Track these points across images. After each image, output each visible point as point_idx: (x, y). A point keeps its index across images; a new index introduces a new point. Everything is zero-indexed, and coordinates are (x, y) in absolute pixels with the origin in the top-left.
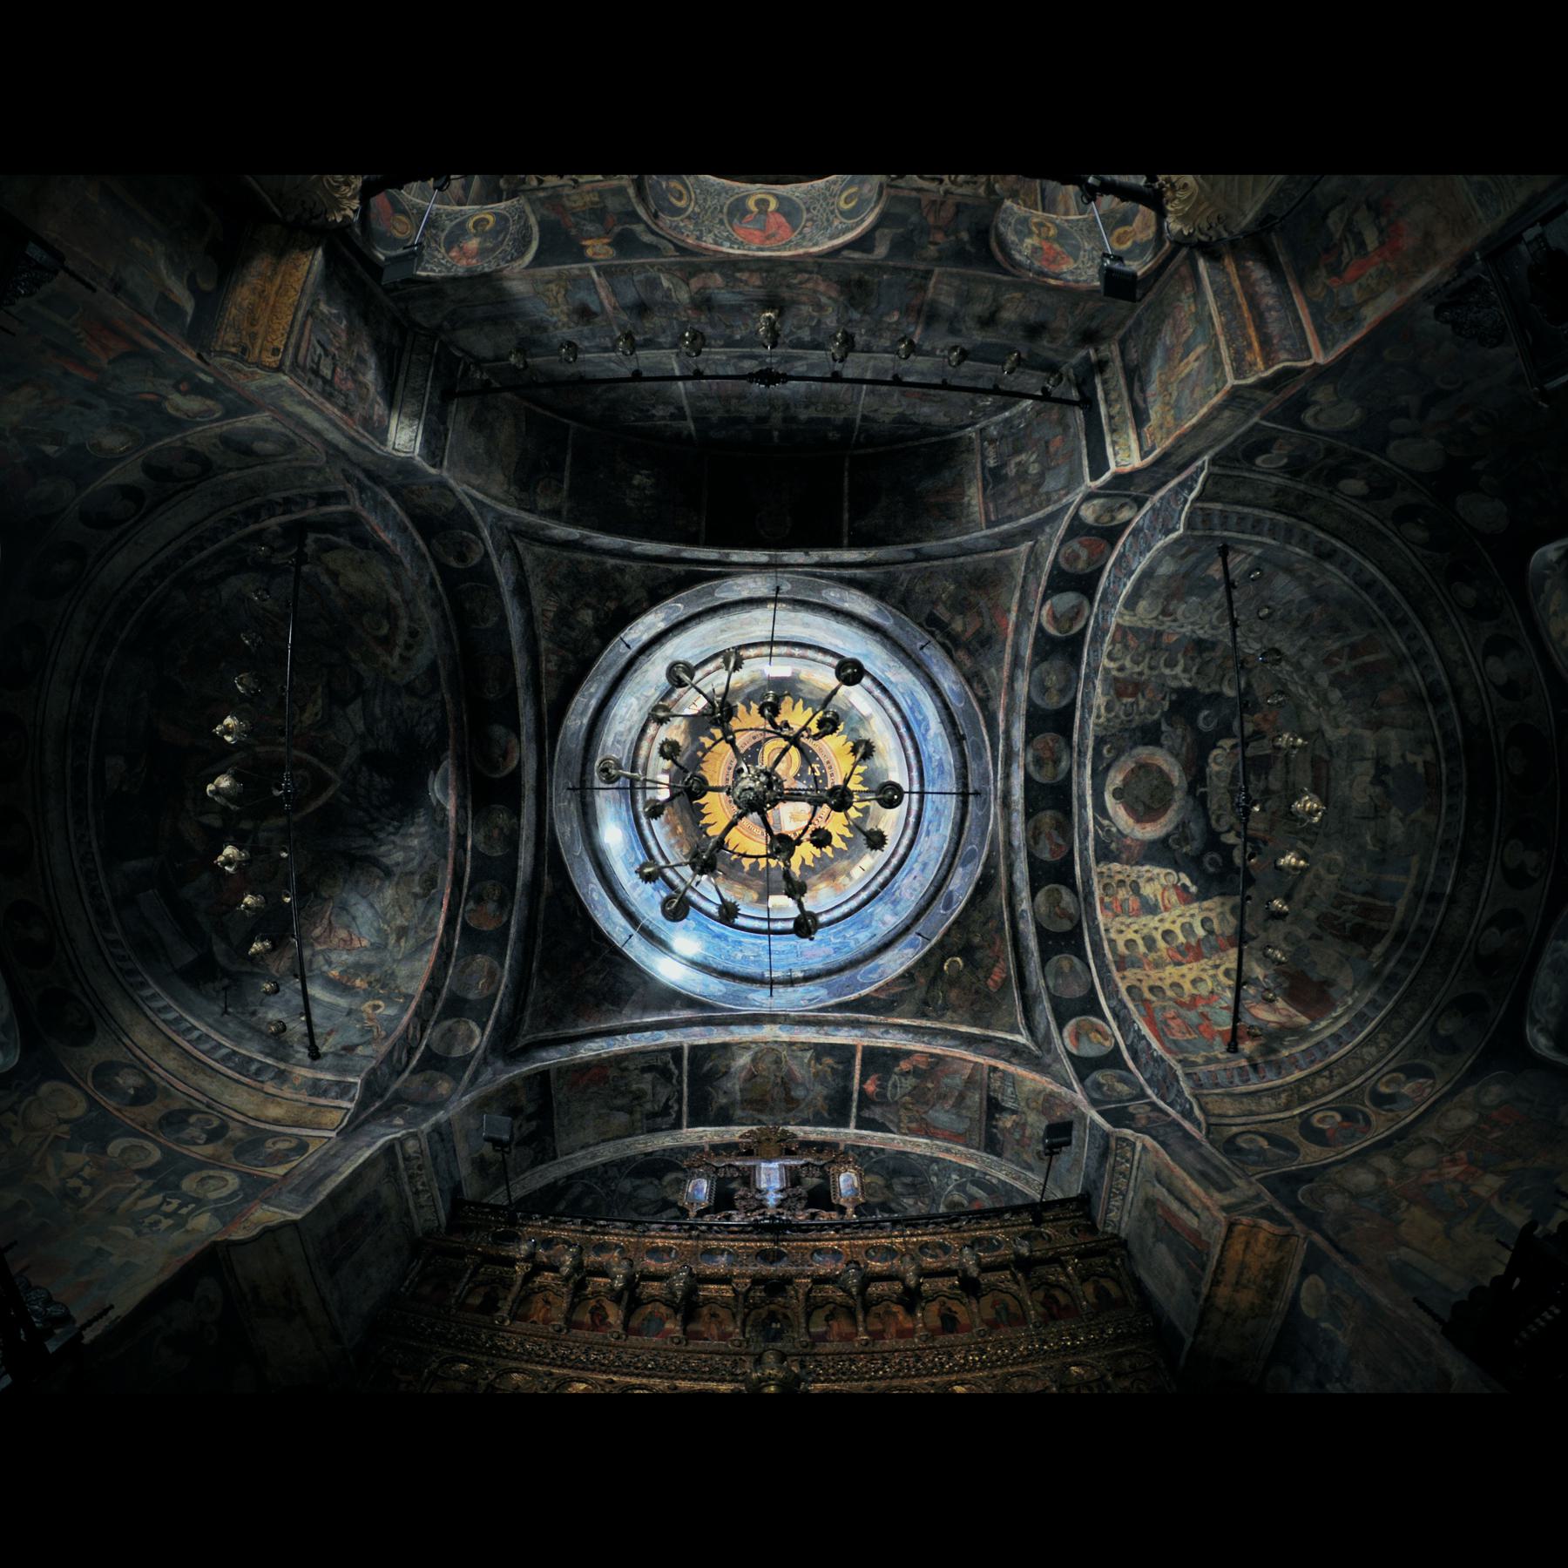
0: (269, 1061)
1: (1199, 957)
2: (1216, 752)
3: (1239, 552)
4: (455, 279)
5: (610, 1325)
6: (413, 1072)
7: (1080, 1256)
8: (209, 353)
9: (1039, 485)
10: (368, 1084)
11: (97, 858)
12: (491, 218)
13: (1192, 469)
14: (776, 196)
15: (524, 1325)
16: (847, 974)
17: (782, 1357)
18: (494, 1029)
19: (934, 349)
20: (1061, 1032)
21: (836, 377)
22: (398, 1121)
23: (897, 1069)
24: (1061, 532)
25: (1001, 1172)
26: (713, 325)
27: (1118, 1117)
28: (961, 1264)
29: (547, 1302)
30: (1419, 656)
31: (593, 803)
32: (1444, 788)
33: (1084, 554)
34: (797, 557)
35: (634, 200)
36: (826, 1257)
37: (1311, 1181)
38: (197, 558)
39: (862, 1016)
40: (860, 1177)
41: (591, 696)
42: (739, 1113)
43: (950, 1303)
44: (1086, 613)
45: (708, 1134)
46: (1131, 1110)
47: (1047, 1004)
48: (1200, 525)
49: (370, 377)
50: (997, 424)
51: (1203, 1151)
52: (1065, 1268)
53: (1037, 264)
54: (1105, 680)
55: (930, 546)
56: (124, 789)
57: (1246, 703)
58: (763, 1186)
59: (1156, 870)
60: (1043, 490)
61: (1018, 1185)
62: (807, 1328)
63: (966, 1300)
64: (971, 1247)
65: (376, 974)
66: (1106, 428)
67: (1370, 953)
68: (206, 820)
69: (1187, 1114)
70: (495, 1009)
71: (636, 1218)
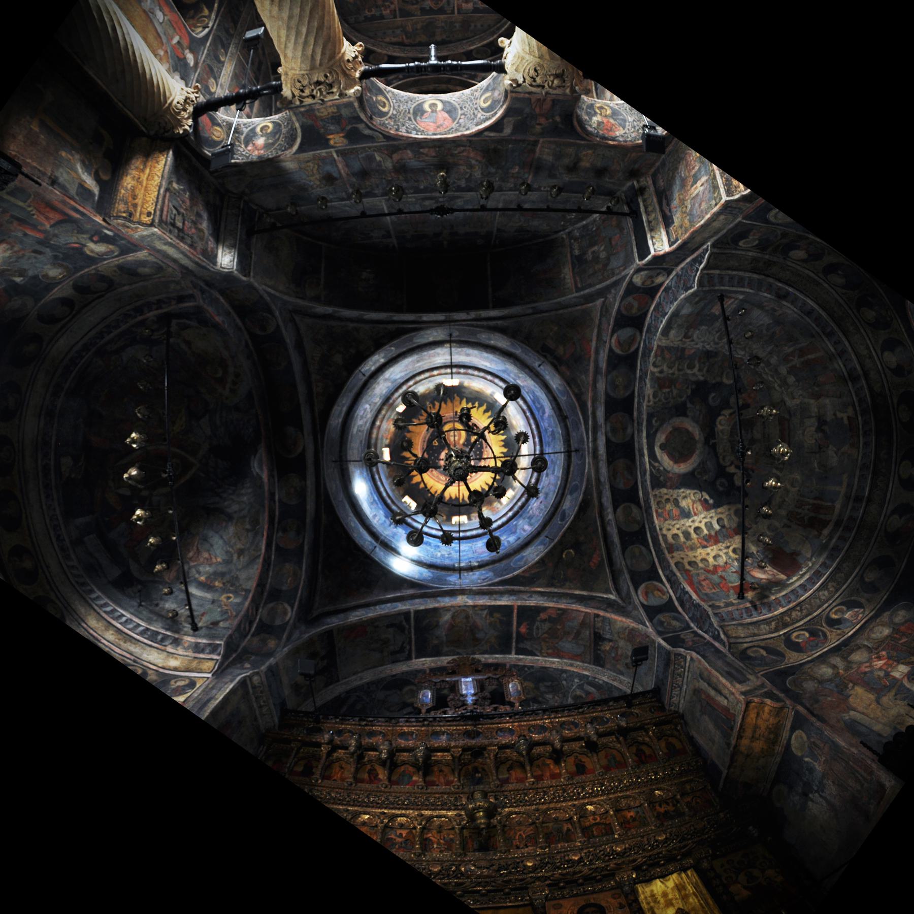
0: (168, 633)
1: (717, 542)
2: (720, 418)
3: (731, 298)
4: (252, 164)
5: (380, 780)
6: (253, 635)
7: (655, 725)
8: (110, 217)
9: (607, 264)
10: (228, 645)
11: (60, 518)
12: (271, 125)
13: (701, 250)
14: (441, 101)
15: (329, 782)
16: (504, 563)
17: (485, 795)
18: (299, 607)
19: (540, 187)
20: (636, 592)
21: (483, 208)
22: (247, 665)
23: (538, 618)
24: (621, 292)
25: (604, 677)
26: (406, 181)
27: (675, 641)
28: (586, 734)
29: (342, 768)
30: (842, 353)
31: (347, 469)
32: (861, 432)
33: (636, 304)
34: (462, 316)
35: (358, 110)
36: (507, 732)
37: (794, 674)
38: (107, 338)
39: (516, 588)
40: (522, 684)
41: (343, 405)
42: (445, 649)
43: (580, 757)
44: (638, 339)
45: (426, 662)
46: (682, 636)
47: (627, 576)
48: (706, 284)
49: (205, 225)
50: (579, 229)
51: (728, 660)
52: (648, 733)
53: (601, 132)
54: (652, 379)
55: (543, 305)
56: (73, 476)
57: (738, 389)
58: (464, 692)
59: (688, 491)
60: (609, 267)
61: (615, 684)
62: (497, 775)
63: (590, 755)
64: (591, 723)
65: (227, 577)
66: (647, 229)
67: (820, 534)
68: (121, 491)
69: (717, 638)
70: (299, 595)
71: (388, 714)
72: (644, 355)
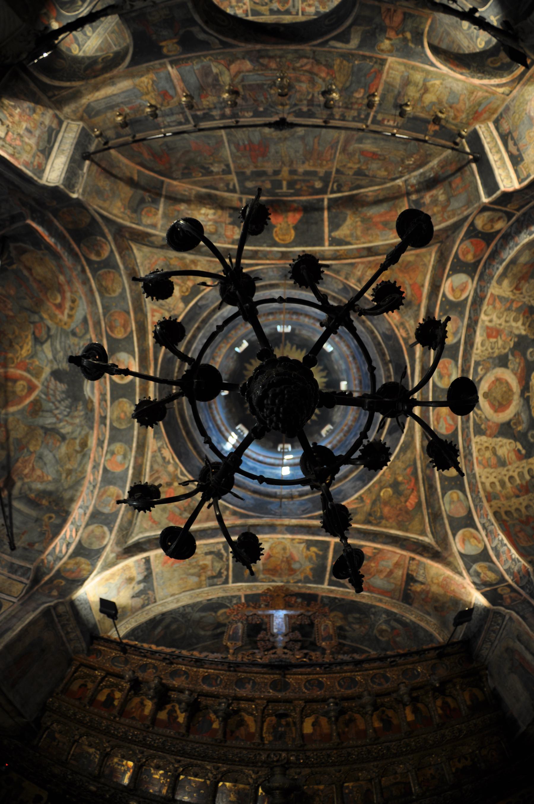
42: (261, 576)
59: (505, 441)
72: (474, 303)
